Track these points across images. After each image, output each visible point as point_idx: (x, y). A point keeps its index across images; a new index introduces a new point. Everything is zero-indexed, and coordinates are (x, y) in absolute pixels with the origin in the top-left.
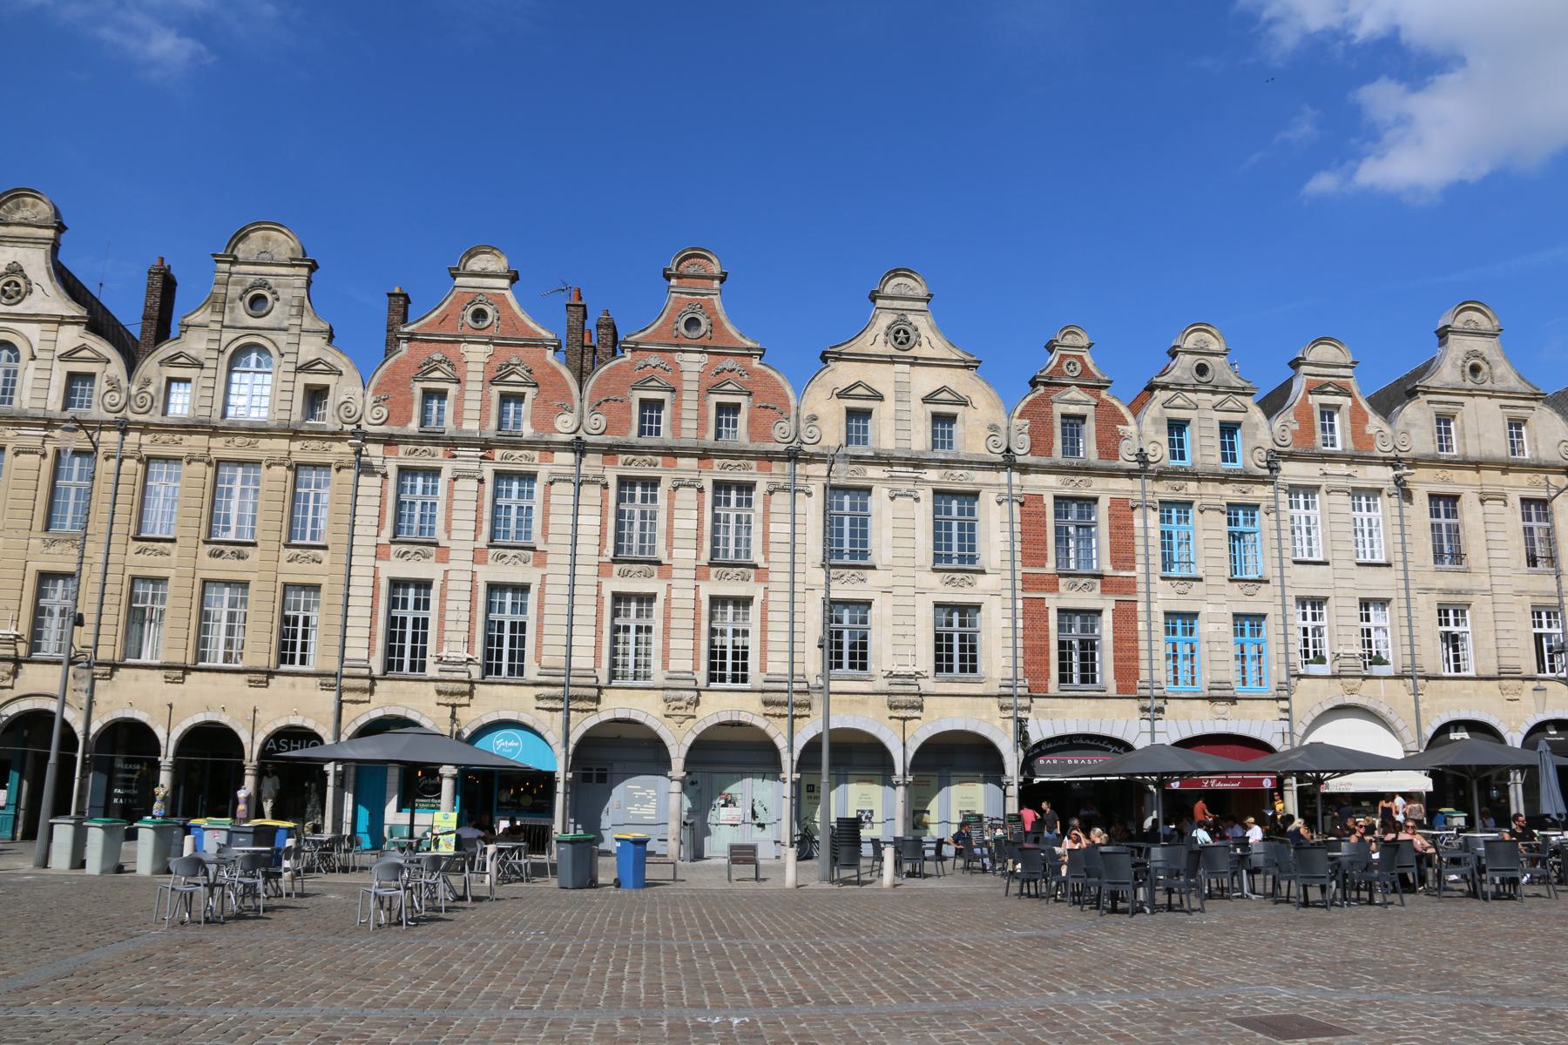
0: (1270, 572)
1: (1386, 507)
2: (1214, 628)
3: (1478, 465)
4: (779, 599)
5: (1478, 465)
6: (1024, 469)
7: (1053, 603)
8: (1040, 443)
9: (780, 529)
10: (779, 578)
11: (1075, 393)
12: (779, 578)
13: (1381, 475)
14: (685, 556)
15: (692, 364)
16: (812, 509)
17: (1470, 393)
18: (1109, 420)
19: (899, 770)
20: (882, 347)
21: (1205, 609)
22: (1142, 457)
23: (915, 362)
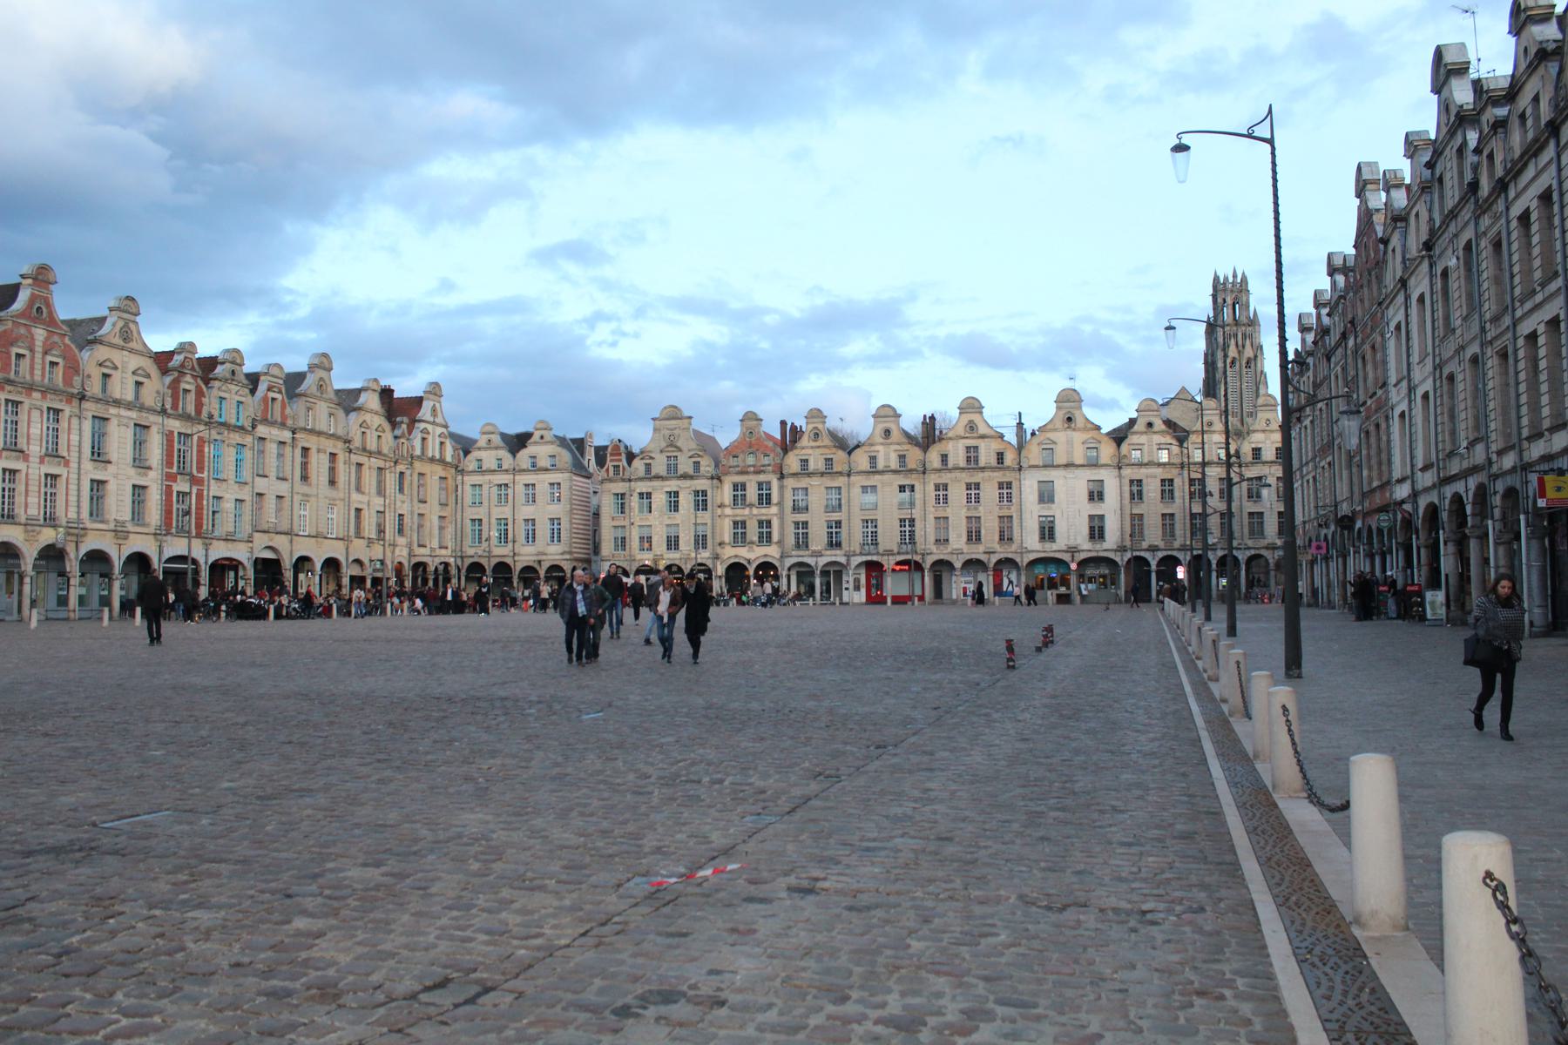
0: (249, 480)
1: (288, 449)
2: (228, 505)
3: (319, 433)
4: (74, 476)
5: (319, 433)
6: (169, 416)
7: (176, 488)
8: (175, 406)
9: (75, 438)
10: (74, 465)
11: (188, 378)
12: (74, 465)
13: (286, 435)
14: (35, 450)
15: (40, 334)
16: (87, 426)
17: (320, 399)
18: (200, 394)
19: (117, 570)
20: (118, 341)
21: (227, 496)
22: (211, 416)
23: (131, 351)
